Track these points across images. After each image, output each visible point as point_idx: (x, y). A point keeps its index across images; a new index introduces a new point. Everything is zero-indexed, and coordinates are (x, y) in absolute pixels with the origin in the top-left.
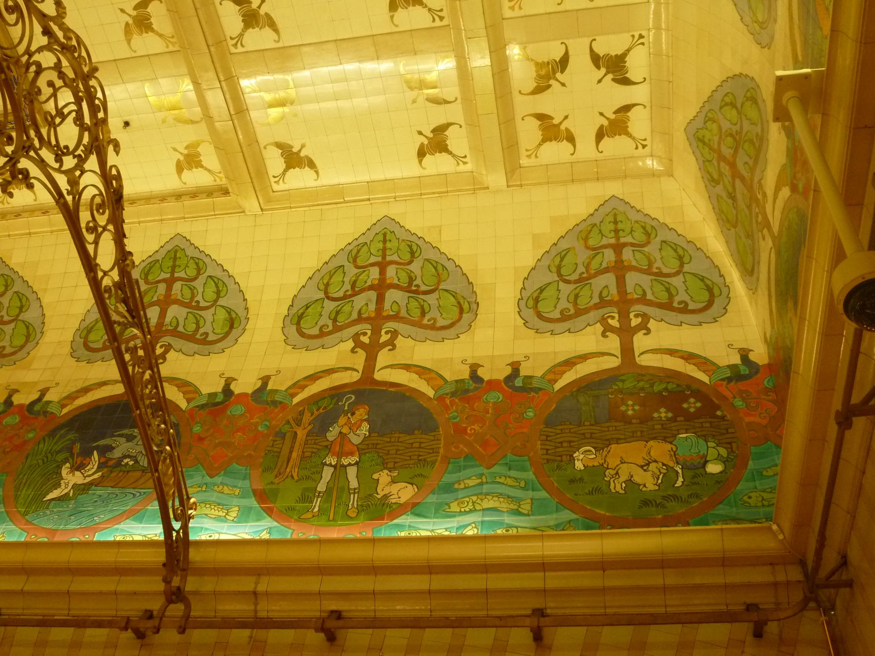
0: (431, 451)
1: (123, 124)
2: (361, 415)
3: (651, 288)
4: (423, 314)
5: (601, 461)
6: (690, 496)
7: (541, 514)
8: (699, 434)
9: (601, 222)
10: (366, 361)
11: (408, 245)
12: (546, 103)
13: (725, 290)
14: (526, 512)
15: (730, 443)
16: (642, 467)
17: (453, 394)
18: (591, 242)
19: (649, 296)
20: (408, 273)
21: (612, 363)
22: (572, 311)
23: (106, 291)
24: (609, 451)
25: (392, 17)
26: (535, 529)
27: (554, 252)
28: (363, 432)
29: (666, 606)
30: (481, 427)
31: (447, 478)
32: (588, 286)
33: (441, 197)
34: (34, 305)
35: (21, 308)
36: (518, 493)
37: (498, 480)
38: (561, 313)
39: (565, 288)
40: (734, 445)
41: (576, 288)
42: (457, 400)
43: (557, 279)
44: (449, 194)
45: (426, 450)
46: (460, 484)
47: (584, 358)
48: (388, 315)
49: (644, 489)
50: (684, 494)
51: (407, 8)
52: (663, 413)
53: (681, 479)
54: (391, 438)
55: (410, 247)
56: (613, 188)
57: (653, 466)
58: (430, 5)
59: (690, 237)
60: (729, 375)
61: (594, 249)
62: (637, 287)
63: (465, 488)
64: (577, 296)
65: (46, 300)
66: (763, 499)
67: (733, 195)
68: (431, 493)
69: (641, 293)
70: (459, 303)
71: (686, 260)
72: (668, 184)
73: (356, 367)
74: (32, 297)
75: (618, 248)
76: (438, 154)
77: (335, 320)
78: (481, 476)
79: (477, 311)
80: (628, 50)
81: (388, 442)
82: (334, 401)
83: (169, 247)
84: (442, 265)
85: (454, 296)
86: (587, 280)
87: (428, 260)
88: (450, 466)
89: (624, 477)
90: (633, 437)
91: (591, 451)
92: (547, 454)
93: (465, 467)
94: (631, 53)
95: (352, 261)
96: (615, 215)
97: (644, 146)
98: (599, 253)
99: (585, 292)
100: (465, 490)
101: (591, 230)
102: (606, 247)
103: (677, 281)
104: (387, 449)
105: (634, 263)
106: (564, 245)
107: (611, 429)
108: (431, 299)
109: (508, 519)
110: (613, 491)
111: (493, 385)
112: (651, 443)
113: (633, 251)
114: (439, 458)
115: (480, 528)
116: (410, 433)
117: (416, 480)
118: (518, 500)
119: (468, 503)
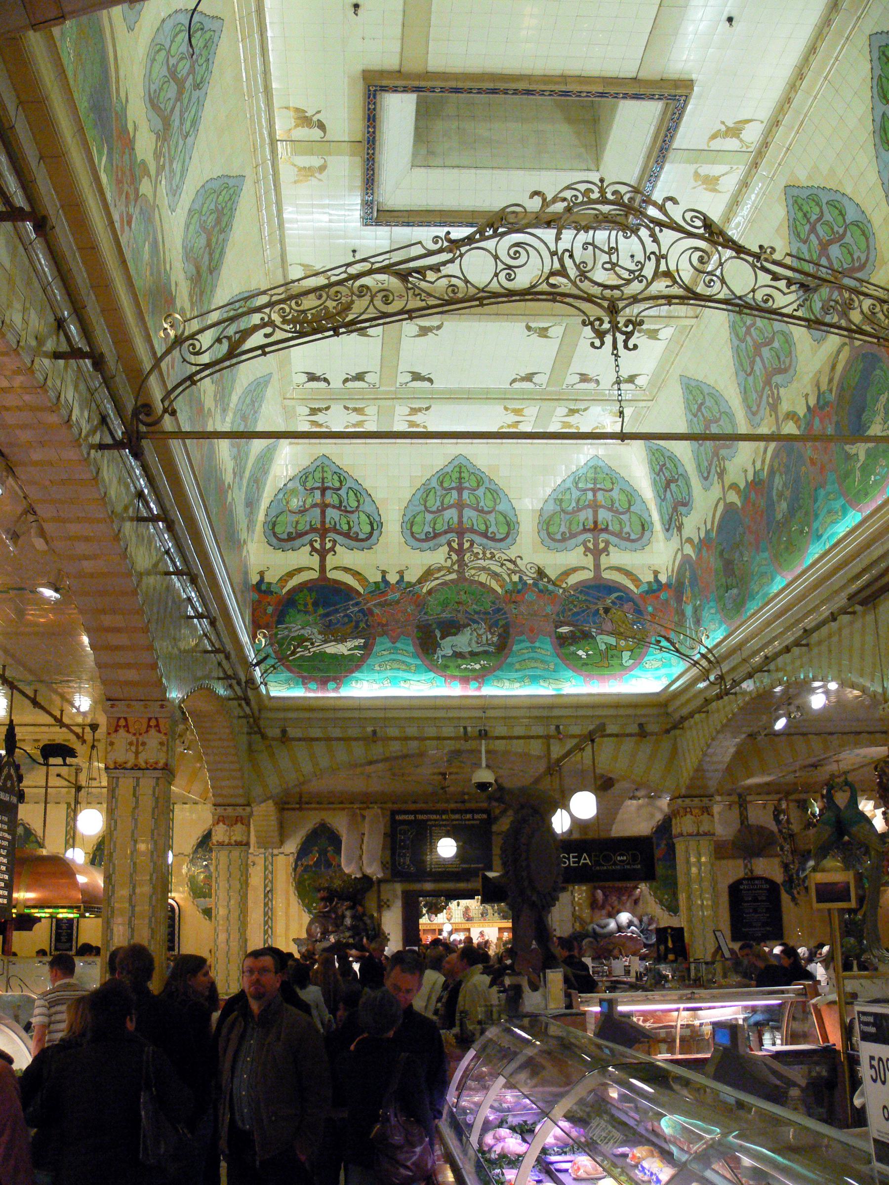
1: (727, 24)
23: (766, 301)
34: (845, 201)
35: (842, 214)
65: (848, 191)
74: (838, 197)
83: (876, 55)
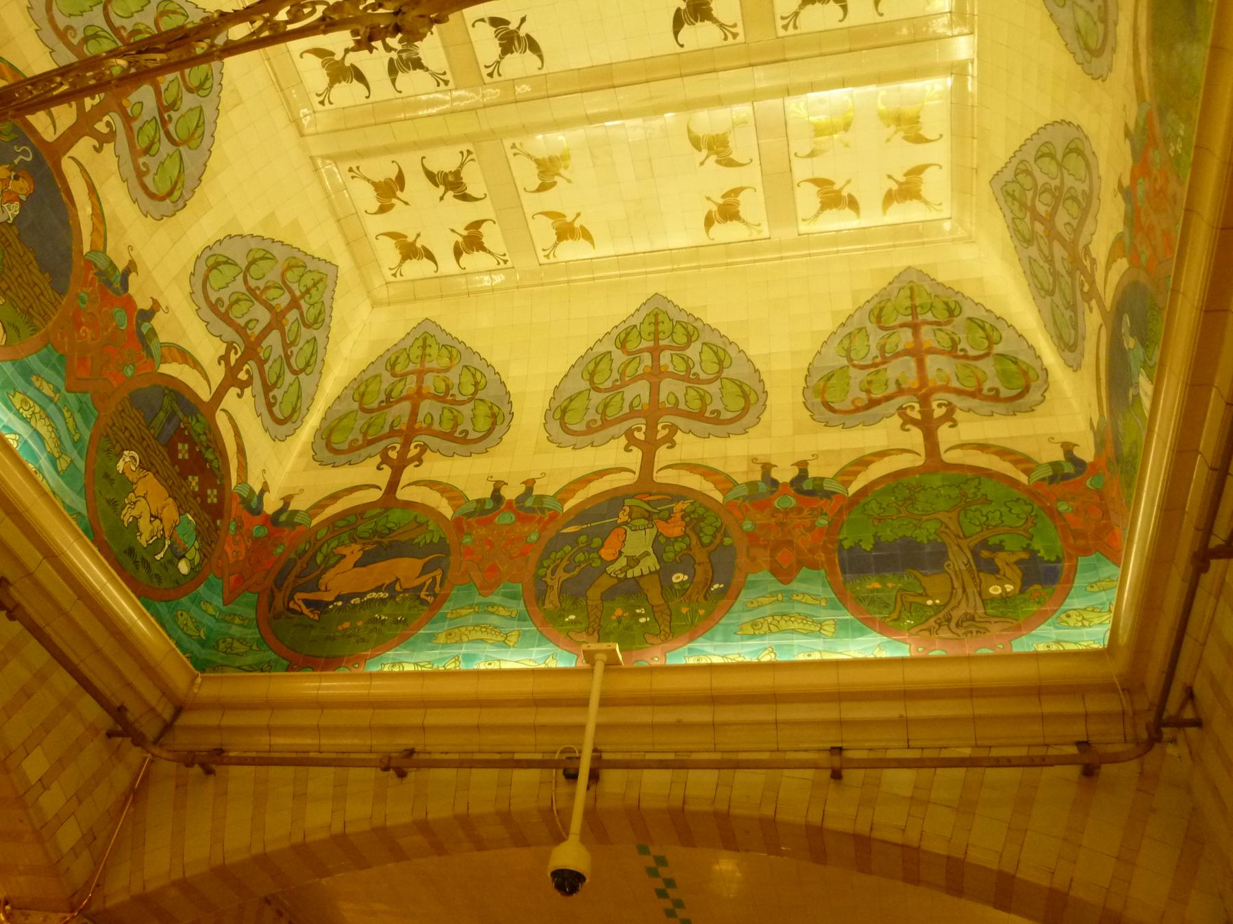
0: (43, 314)
2: (21, 189)
3: (275, 361)
4: (147, 151)
5: (135, 481)
6: (156, 575)
7: (67, 483)
8: (198, 527)
9: (310, 271)
10: (69, 128)
11: (207, 75)
12: (417, 185)
13: (299, 422)
14: (60, 469)
15: (205, 556)
16: (152, 516)
17: (100, 273)
18: (290, 275)
19: (266, 367)
20: (178, 95)
21: (205, 394)
22: (223, 310)
24: (145, 476)
25: (482, 20)
26: (54, 493)
27: (264, 245)
28: (10, 213)
29: (82, 661)
30: (93, 339)
31: (34, 361)
32: (250, 304)
33: (274, 84)
36: (68, 444)
37: (64, 411)
38: (219, 300)
39: (239, 286)
40: (206, 560)
41: (243, 294)
42: (97, 284)
43: (243, 268)
44: (280, 93)
45: (40, 309)
46: (38, 380)
47: (196, 365)
48: (125, 107)
49: (138, 538)
50: (155, 570)
51: (496, 37)
52: (194, 481)
53: (161, 555)
54: (25, 253)
55: (207, 78)
56: (343, 261)
57: (158, 521)
58: (503, 62)
59: (328, 358)
60: (245, 496)
61: (284, 282)
62: (269, 349)
63: (39, 390)
64: (237, 301)
66: (186, 625)
67: (392, 400)
68: (11, 360)
69: (267, 356)
70: (176, 183)
71: (309, 370)
72: (364, 309)
73: (58, 122)
75: (294, 304)
76: (325, 72)
77: (86, 40)
78: (57, 390)
79: (178, 211)
80: (490, 252)
81: (20, 255)
82: (13, 136)
84: (203, 133)
85: (180, 171)
86: (255, 298)
87: (201, 110)
88: (45, 350)
89: (135, 513)
90: (163, 480)
91: (136, 462)
92: (111, 428)
93: (54, 368)
94: (488, 255)
95: (159, 10)
96: (321, 280)
97: (394, 275)
98: (282, 289)
99: (244, 305)
100: (36, 391)
101: (299, 267)
102: (291, 291)
103: (289, 377)
104: (14, 262)
105: (287, 328)
106: (276, 250)
107: (161, 456)
108: (165, 147)
109: (44, 462)
110: (122, 516)
111: (129, 303)
112: (171, 500)
113: (297, 319)
114: (43, 330)
115: (20, 445)
116: (43, 269)
117: (11, 331)
118: (63, 451)
119: (30, 408)
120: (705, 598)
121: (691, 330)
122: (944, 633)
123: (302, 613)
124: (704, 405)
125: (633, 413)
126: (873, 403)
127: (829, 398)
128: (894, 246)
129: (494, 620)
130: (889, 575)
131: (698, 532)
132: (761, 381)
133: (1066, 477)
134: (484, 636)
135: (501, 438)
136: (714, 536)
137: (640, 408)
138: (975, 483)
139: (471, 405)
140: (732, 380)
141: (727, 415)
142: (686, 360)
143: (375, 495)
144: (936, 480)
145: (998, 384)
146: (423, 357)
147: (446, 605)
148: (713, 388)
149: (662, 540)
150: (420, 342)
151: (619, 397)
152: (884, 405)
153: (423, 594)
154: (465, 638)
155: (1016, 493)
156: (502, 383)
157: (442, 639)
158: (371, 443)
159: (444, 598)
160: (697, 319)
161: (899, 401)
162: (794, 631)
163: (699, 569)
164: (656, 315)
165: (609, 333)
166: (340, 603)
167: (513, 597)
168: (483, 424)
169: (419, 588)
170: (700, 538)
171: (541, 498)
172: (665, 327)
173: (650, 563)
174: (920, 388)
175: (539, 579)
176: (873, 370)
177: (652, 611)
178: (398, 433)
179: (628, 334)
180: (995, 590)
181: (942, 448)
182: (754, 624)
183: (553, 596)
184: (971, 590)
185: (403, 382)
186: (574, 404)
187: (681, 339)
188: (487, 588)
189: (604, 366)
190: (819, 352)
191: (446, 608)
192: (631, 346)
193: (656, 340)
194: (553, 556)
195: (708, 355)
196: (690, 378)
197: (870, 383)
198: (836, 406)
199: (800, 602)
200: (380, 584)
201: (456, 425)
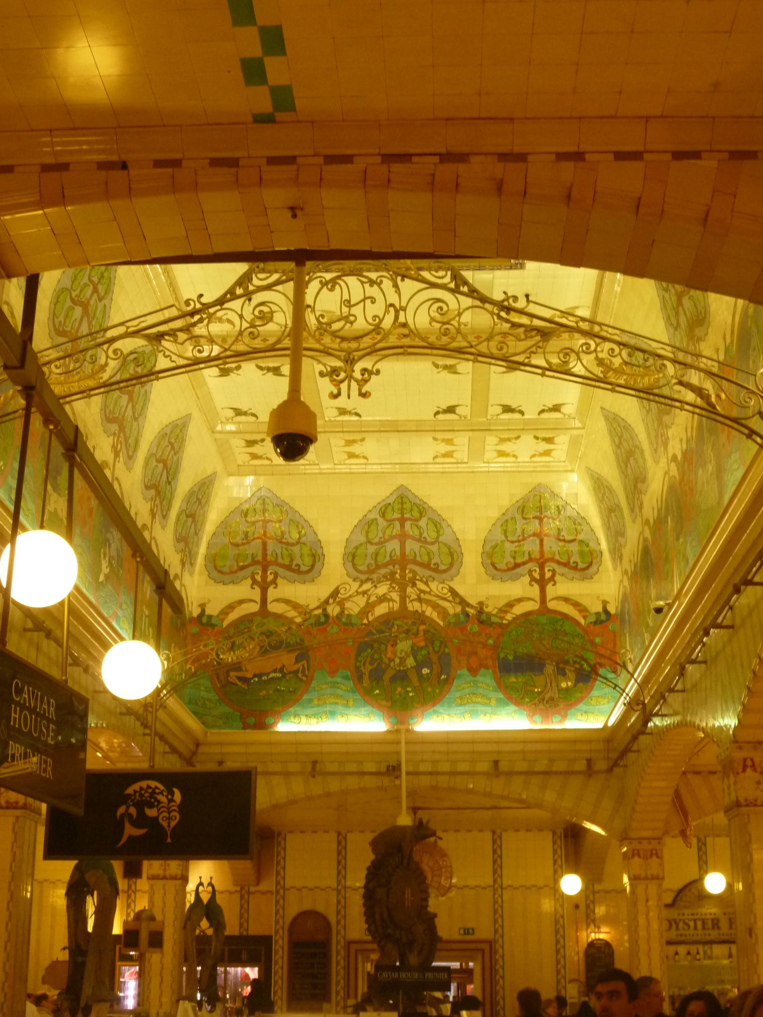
120: (439, 683)
121: (422, 509)
122: (541, 706)
123: (237, 685)
124: (430, 560)
125: (392, 562)
126: (517, 566)
127: (494, 561)
128: (534, 471)
129: (339, 692)
130: (520, 674)
131: (432, 643)
132: (460, 546)
133: (602, 622)
134: (337, 701)
135: (320, 572)
136: (440, 646)
137: (395, 558)
138: (561, 623)
139: (298, 547)
140: (445, 544)
141: (442, 567)
142: (419, 527)
143: (255, 608)
144: (543, 620)
145: (578, 560)
146: (264, 511)
147: (313, 682)
148: (434, 548)
149: (415, 647)
150: (261, 501)
151: (383, 550)
152: (522, 568)
153: (300, 675)
154: (327, 702)
155: (579, 631)
156: (315, 533)
157: (316, 702)
158: (242, 568)
159: (312, 678)
160: (425, 503)
161: (530, 566)
162: (478, 703)
163: (434, 666)
164: (402, 498)
165: (375, 507)
166: (256, 679)
167: (346, 678)
168: (308, 561)
169: (296, 672)
170: (434, 649)
171: (349, 616)
172: (407, 506)
173: (410, 662)
174: (540, 559)
175: (358, 669)
176: (517, 544)
177: (415, 689)
178: (258, 562)
179: (386, 508)
180: (564, 685)
181: (548, 598)
182: (461, 698)
183: (366, 678)
184: (554, 684)
185: (254, 527)
186: (359, 551)
187: (416, 514)
188: (333, 673)
189: (373, 527)
190: (490, 530)
191: (314, 684)
192: (389, 516)
193: (402, 514)
194: (362, 654)
195: (431, 526)
196: (421, 540)
197: (515, 552)
198: (498, 566)
199: (481, 687)
200: (275, 668)
201: (292, 560)
